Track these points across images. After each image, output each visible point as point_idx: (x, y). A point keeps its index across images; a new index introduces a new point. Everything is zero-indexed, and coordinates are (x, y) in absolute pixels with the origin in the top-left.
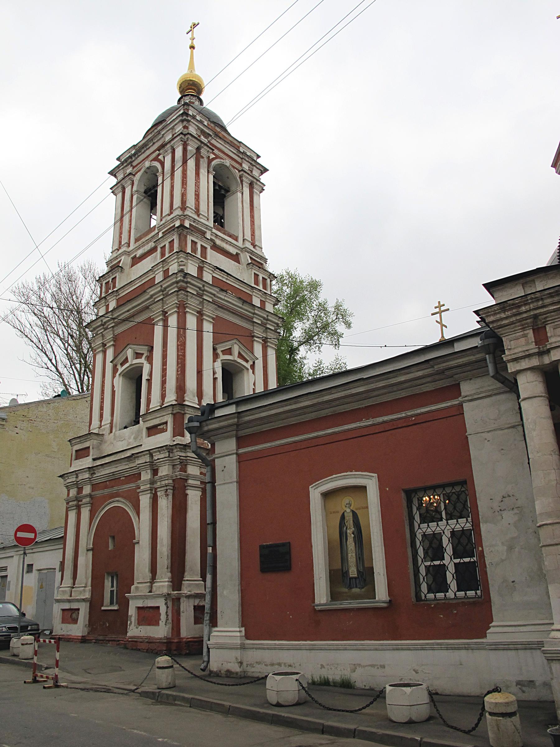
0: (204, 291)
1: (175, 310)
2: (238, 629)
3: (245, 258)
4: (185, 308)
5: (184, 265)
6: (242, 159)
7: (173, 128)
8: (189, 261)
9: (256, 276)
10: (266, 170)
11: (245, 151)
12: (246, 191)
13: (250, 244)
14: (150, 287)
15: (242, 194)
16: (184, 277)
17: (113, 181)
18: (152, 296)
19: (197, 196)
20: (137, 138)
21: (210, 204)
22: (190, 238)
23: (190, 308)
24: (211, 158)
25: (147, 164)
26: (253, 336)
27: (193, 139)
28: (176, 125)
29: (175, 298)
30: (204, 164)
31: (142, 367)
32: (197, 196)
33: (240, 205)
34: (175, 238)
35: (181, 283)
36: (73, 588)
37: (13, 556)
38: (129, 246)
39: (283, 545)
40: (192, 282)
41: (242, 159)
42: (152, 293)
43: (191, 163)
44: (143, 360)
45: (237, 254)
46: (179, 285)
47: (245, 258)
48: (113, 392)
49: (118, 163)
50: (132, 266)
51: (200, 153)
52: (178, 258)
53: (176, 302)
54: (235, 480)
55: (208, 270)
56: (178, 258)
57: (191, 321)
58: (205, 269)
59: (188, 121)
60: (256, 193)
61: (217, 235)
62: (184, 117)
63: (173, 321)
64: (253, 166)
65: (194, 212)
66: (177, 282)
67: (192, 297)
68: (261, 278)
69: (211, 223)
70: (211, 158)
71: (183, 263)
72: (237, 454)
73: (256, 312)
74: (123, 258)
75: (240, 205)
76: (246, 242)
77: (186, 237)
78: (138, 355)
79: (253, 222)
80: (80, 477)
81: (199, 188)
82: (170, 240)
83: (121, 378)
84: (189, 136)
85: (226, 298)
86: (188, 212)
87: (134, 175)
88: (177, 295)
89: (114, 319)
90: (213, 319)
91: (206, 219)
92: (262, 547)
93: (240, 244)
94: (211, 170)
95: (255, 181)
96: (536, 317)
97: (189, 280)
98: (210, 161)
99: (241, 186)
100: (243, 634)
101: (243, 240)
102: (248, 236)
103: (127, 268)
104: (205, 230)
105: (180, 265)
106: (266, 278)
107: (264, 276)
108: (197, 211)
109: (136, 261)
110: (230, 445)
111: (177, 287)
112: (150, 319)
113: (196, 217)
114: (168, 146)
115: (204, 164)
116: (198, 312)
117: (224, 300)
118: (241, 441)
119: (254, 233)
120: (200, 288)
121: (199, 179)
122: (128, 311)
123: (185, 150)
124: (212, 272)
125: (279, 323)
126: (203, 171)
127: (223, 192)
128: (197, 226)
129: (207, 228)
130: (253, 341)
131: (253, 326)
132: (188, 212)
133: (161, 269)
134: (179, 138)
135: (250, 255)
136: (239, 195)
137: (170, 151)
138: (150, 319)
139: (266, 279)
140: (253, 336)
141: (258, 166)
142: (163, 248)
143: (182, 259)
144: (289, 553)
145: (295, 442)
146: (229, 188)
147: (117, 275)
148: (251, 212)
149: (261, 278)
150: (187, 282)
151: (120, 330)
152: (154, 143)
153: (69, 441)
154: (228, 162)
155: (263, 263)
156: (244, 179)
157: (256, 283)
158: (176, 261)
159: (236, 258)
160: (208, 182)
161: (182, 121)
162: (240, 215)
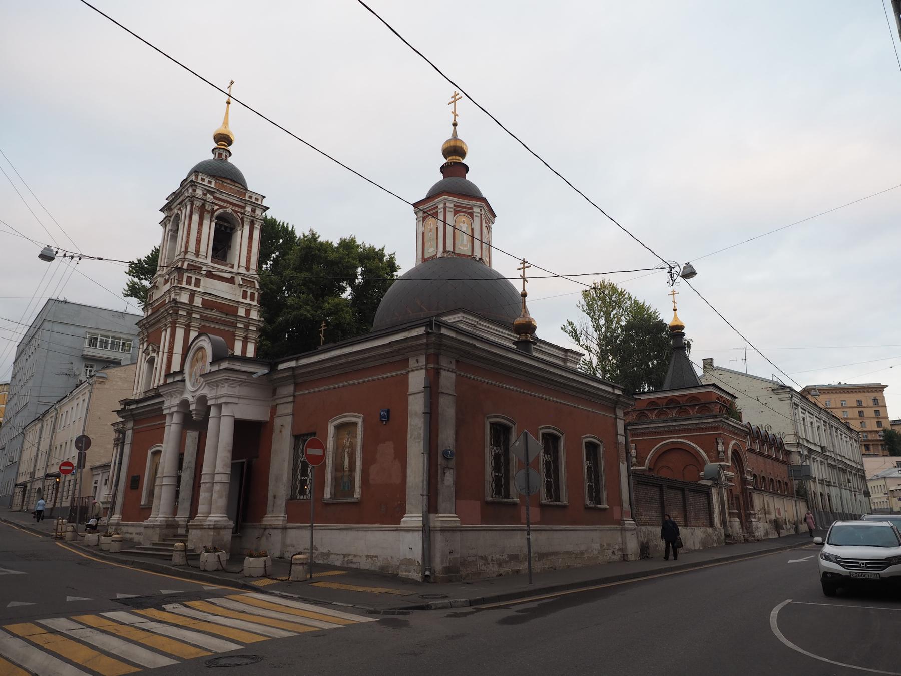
0: (192, 311)
1: (170, 325)
2: (118, 516)
3: (239, 280)
4: (176, 324)
5: (178, 295)
6: (245, 203)
7: (187, 189)
8: (183, 292)
9: (245, 293)
10: (268, 208)
12: (247, 229)
13: (244, 269)
14: (160, 308)
15: (242, 232)
16: (175, 304)
17: (162, 216)
18: (162, 313)
19: (198, 242)
20: (176, 187)
21: (209, 245)
22: (185, 275)
23: (178, 324)
24: (215, 209)
25: (176, 212)
26: (235, 336)
27: (198, 200)
28: (189, 187)
29: (170, 318)
30: (207, 217)
31: (154, 358)
32: (198, 242)
33: (239, 240)
34: (176, 274)
35: (175, 308)
36: (109, 495)
37: (99, 474)
38: (163, 271)
39: (137, 476)
40: (182, 306)
41: (245, 203)
42: (162, 311)
43: (196, 218)
44: (155, 354)
45: (232, 278)
46: (173, 308)
47: (239, 280)
48: (143, 372)
49: (167, 202)
50: (165, 285)
51: (205, 207)
52: (175, 290)
53: (170, 320)
54: (130, 442)
55: (198, 296)
56: (175, 290)
57: (180, 333)
58: (196, 295)
59: (196, 186)
60: (256, 227)
61: (213, 268)
62: (192, 184)
63: (169, 331)
64: (256, 207)
65: (194, 255)
66: (171, 307)
67: (181, 317)
68: (249, 294)
69: (208, 261)
70: (215, 209)
71: (176, 294)
72: (132, 429)
73: (238, 319)
74: (159, 279)
75: (239, 240)
76: (241, 268)
77: (183, 274)
78: (154, 351)
79: (251, 251)
80: (119, 427)
81: (201, 235)
82: (174, 276)
83: (147, 364)
84: (194, 198)
85: (211, 313)
86: (188, 256)
87: (171, 217)
88: (171, 316)
89: (148, 323)
90: (199, 329)
91: (204, 258)
92: (133, 477)
93: (235, 270)
94: (214, 219)
95: (255, 219)
96: (170, 392)
97: (179, 306)
98: (213, 212)
99: (241, 226)
100: (120, 519)
101: (239, 267)
102: (243, 262)
103: (160, 286)
104: (201, 266)
105: (176, 295)
106: (255, 292)
107: (252, 291)
108: (197, 254)
109: (166, 282)
110: (130, 424)
111: (172, 310)
112: (160, 328)
113: (194, 259)
114: (183, 203)
115: (207, 217)
116: (185, 326)
117: (210, 315)
118: (136, 422)
119: (250, 259)
120: (188, 309)
121: (202, 227)
122: (154, 319)
123: (192, 207)
124: (202, 297)
125: (259, 324)
126: (206, 223)
127: (228, 231)
128: (194, 264)
129: (203, 265)
130: (235, 339)
131: (236, 329)
132: (188, 256)
133: (168, 296)
134: (187, 200)
135: (242, 277)
136: (239, 233)
137: (185, 207)
138: (160, 328)
139: (254, 294)
140: (235, 336)
141: (259, 207)
142: (171, 279)
143: (177, 291)
144: (138, 480)
145: (149, 426)
146: (235, 226)
147: (154, 291)
148: (249, 243)
149: (249, 294)
150: (178, 307)
151: (150, 331)
152: (180, 197)
153: (119, 401)
154: (229, 211)
155: (254, 281)
156: (245, 219)
157: (245, 297)
158: (173, 292)
159: (231, 281)
160: (210, 229)
161: (191, 186)
162: (238, 248)
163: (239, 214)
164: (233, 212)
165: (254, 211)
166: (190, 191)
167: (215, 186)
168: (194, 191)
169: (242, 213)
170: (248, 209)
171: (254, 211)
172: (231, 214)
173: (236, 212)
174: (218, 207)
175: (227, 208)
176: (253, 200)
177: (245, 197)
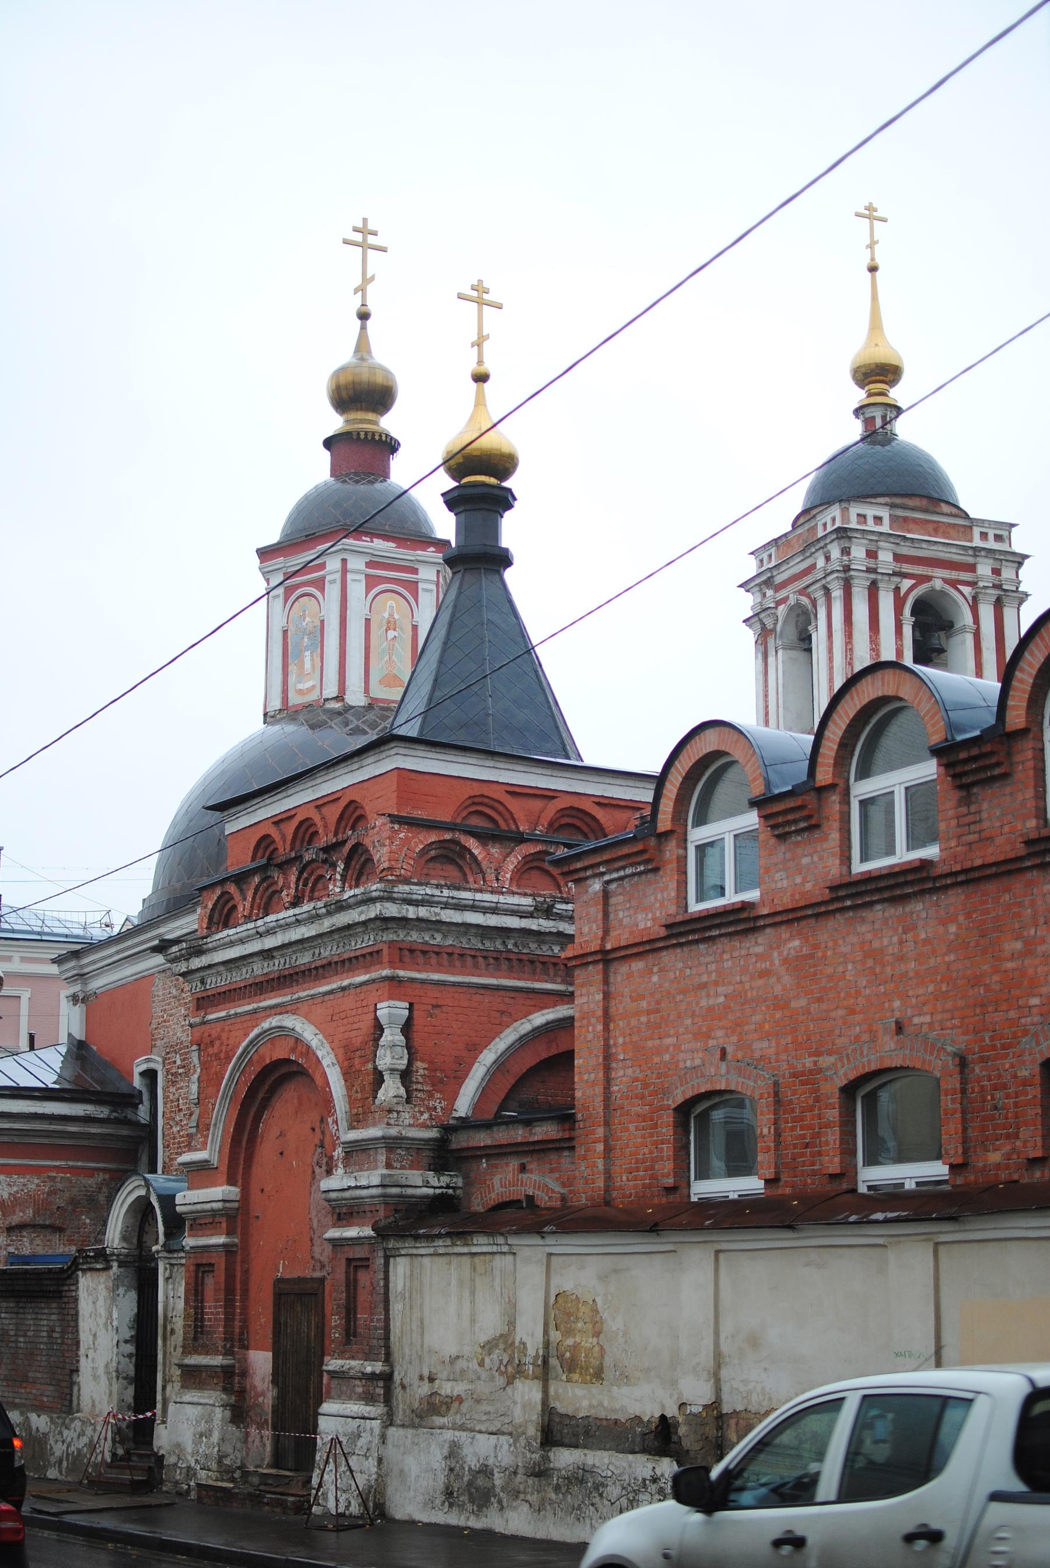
11: (984, 530)
154: (938, 584)
163: (960, 587)
164: (947, 587)
165: (996, 572)
166: (835, 553)
167: (891, 528)
168: (846, 551)
169: (972, 584)
170: (984, 569)
171: (996, 572)
172: (943, 593)
173: (954, 583)
174: (913, 582)
175: (928, 579)
176: (991, 544)
177: (971, 541)
